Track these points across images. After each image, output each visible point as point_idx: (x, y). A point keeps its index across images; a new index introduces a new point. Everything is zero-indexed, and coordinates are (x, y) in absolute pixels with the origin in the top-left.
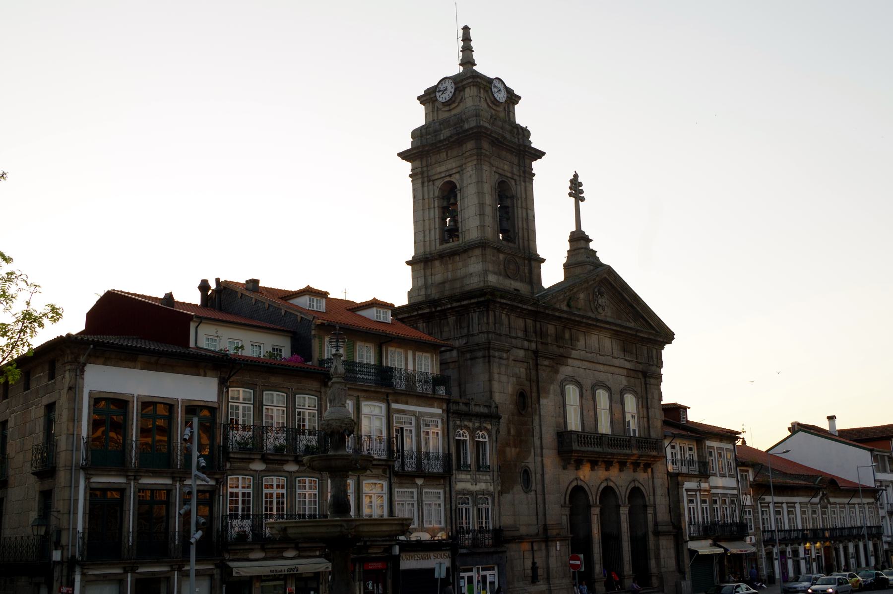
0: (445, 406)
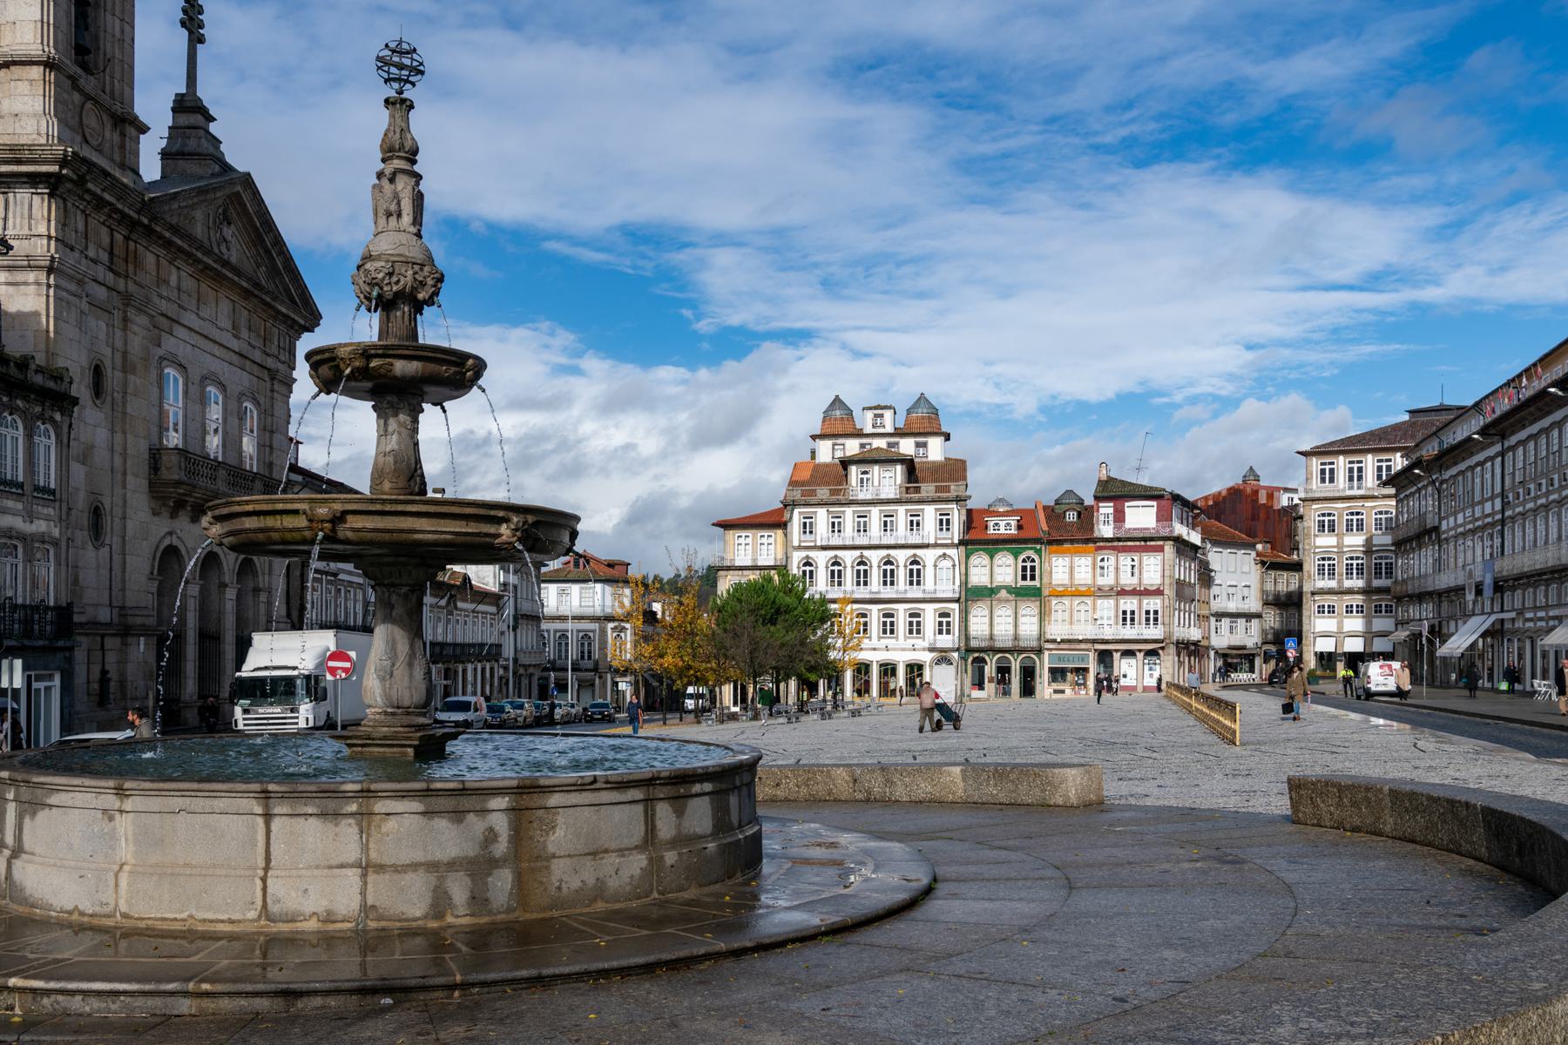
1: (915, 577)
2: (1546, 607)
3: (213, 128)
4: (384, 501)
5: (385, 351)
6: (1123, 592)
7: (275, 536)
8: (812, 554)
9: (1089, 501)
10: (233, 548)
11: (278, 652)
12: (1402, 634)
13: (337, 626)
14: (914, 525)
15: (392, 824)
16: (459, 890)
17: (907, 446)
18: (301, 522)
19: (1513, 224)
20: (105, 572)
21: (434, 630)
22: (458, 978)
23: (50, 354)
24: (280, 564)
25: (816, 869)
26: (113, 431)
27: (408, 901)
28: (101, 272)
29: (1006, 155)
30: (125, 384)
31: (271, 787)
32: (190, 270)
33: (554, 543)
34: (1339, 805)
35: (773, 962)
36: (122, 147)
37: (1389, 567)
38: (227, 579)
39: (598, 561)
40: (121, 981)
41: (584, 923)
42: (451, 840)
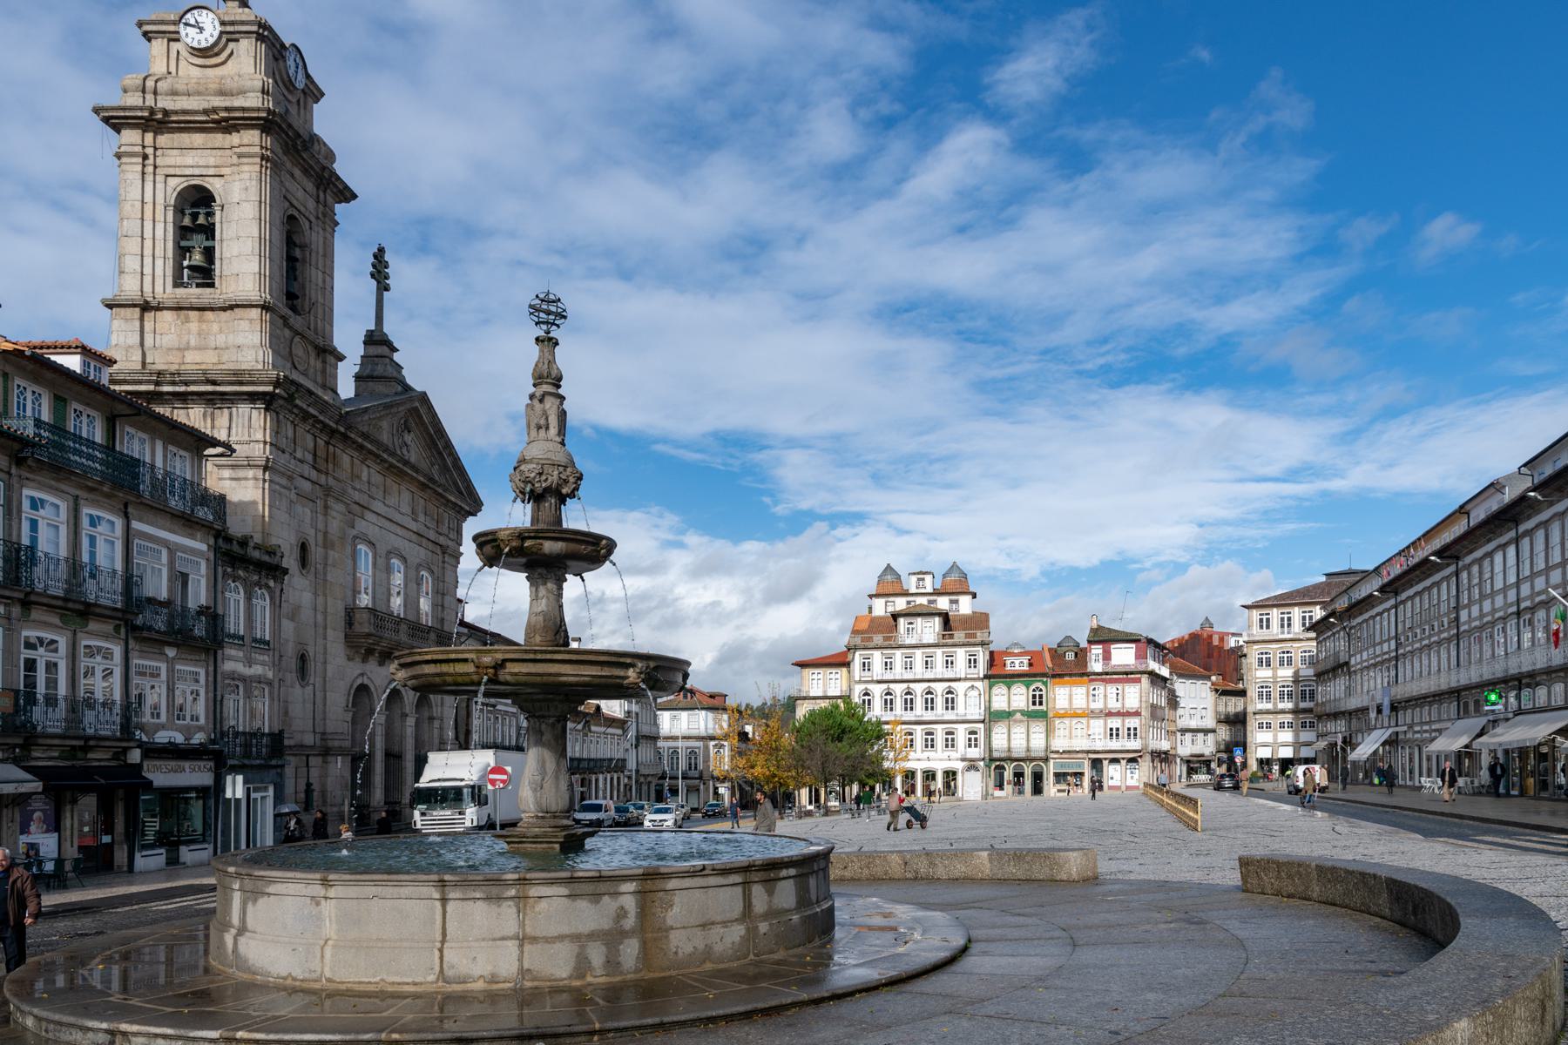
0: (212, 542)
1: (950, 704)
2: (1430, 722)
3: (396, 357)
4: (535, 652)
5: (536, 534)
6: (1110, 714)
7: (449, 679)
8: (870, 686)
9: (1084, 644)
10: (414, 689)
11: (448, 767)
12: (1322, 744)
13: (495, 746)
14: (949, 663)
15: (543, 904)
16: (597, 954)
17: (943, 603)
18: (470, 668)
19: (1397, 431)
20: (309, 706)
21: (575, 749)
22: (597, 1026)
23: (266, 534)
24: (450, 701)
25: (877, 934)
26: (316, 594)
27: (556, 965)
28: (307, 470)
29: (1011, 379)
30: (326, 558)
31: (447, 877)
32: (378, 468)
33: (671, 683)
34: (1278, 878)
35: (845, 1008)
36: (324, 371)
37: (1312, 693)
38: (407, 710)
39: (702, 694)
40: (327, 1032)
41: (696, 980)
42: (590, 916)
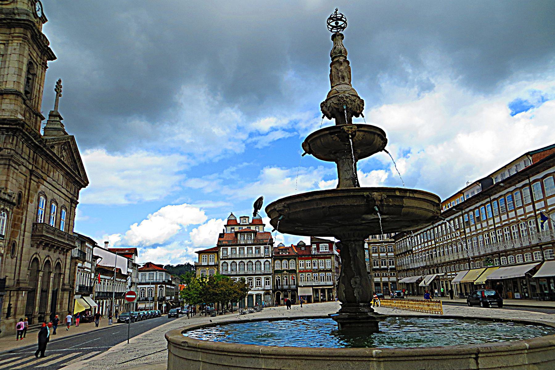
17: (253, 228)
